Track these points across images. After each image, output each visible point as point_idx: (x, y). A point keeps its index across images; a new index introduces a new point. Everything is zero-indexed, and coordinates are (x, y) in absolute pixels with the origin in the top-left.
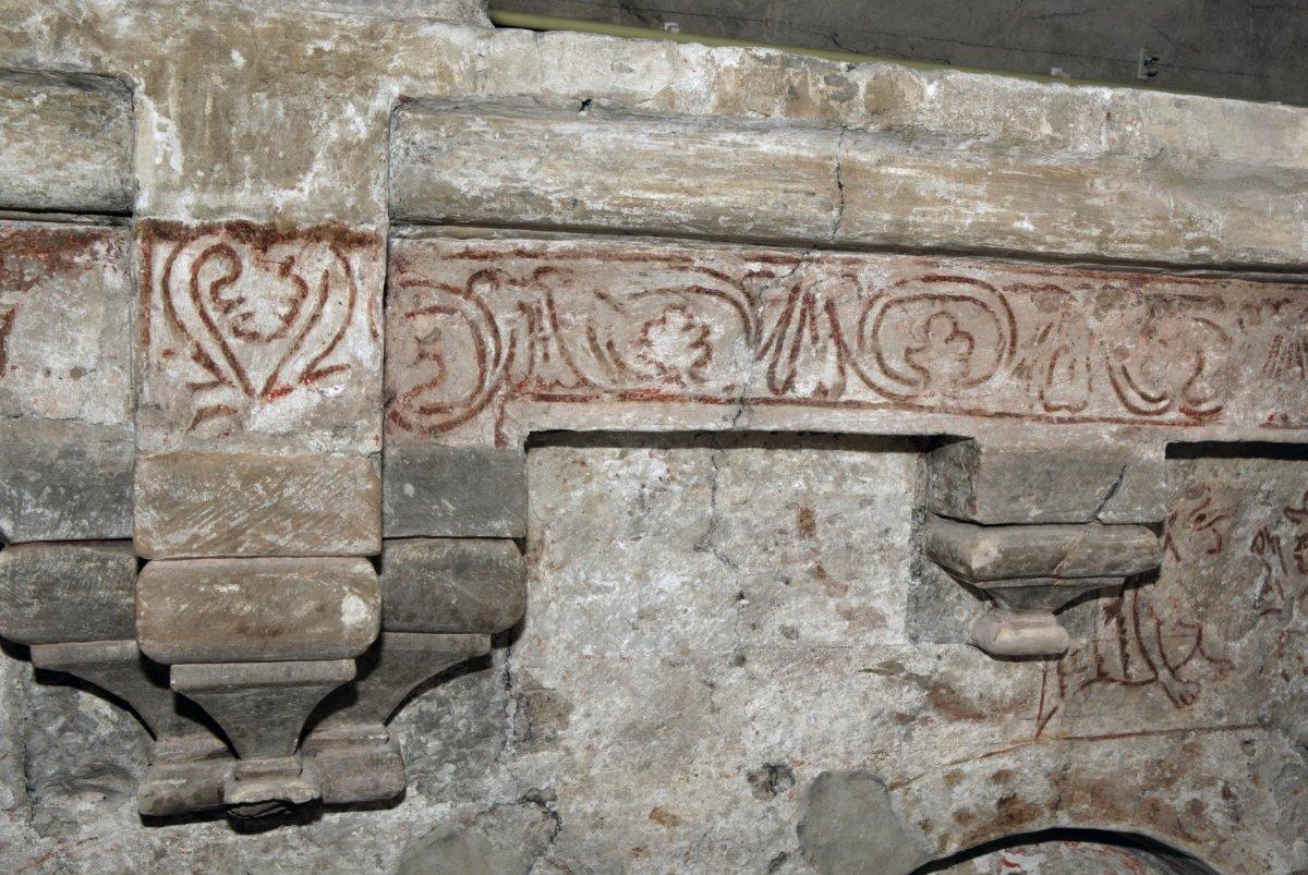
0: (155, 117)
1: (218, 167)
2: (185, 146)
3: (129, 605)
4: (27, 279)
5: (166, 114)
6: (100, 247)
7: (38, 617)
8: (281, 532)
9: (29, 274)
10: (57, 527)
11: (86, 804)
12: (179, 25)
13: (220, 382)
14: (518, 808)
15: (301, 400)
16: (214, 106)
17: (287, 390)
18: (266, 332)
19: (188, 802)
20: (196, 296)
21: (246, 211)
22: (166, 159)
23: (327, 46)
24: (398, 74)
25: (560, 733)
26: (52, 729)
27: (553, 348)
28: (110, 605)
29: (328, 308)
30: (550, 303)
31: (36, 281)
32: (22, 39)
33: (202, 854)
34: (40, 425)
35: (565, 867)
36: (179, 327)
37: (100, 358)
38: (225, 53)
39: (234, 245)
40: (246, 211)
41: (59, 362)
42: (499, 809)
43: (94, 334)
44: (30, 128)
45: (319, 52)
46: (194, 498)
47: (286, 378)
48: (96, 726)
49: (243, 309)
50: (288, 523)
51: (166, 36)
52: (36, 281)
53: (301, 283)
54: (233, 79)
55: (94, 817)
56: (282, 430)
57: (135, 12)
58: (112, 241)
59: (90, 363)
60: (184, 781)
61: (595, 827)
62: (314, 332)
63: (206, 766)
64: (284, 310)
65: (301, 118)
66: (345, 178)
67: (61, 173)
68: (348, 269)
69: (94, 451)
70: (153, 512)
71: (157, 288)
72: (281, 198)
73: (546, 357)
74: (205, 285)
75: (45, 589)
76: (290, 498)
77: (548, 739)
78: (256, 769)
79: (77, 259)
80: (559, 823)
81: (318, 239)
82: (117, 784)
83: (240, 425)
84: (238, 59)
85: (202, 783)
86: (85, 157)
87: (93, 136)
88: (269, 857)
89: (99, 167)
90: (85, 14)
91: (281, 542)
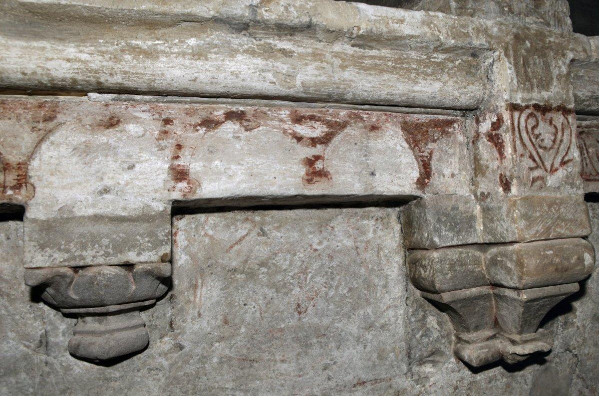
0: (507, 64)
1: (527, 83)
2: (517, 75)
3: (479, 271)
4: (436, 138)
5: (510, 63)
6: (456, 125)
7: (451, 279)
8: (561, 227)
9: (436, 135)
10: (453, 240)
11: (428, 369)
12: (511, 31)
13: (537, 167)
14: (565, 354)
15: (561, 173)
16: (523, 61)
17: (557, 170)
18: (549, 146)
19: (490, 359)
20: (527, 132)
21: (536, 100)
22: (512, 81)
23: (552, 39)
24: (572, 50)
25: (574, 320)
26: (418, 336)
27: (588, 161)
28: (473, 272)
29: (565, 137)
30: (585, 144)
31: (438, 139)
32: (467, 35)
33: (469, 386)
34: (444, 197)
35: (582, 378)
36: (524, 145)
37: (459, 169)
38: (524, 41)
39: (536, 113)
40: (536, 100)
41: (447, 172)
42: (559, 354)
43: (457, 160)
44: (455, 73)
45: (550, 41)
46: (534, 215)
47: (557, 165)
48: (432, 333)
49: (541, 137)
50: (563, 224)
51: (507, 35)
52: (438, 139)
53: (556, 127)
54: (527, 50)
55: (433, 374)
56: (557, 185)
57: (498, 26)
58: (459, 123)
59: (456, 172)
60: (487, 350)
61: (588, 359)
62: (562, 146)
63: (490, 343)
64: (553, 138)
65: (547, 65)
66: (562, 88)
67: (466, 90)
68: (568, 121)
69: (462, 207)
70: (524, 221)
71: (517, 129)
72: (546, 95)
73: (587, 164)
74: (529, 128)
75: (452, 266)
76: (562, 213)
77: (572, 324)
78: (526, 339)
79: (450, 130)
80: (578, 359)
81: (558, 110)
82: (437, 358)
83: (545, 184)
84: (528, 44)
85: (493, 350)
86: (473, 84)
87: (473, 76)
88: (490, 385)
89: (477, 88)
90: (484, 26)
91: (562, 232)
